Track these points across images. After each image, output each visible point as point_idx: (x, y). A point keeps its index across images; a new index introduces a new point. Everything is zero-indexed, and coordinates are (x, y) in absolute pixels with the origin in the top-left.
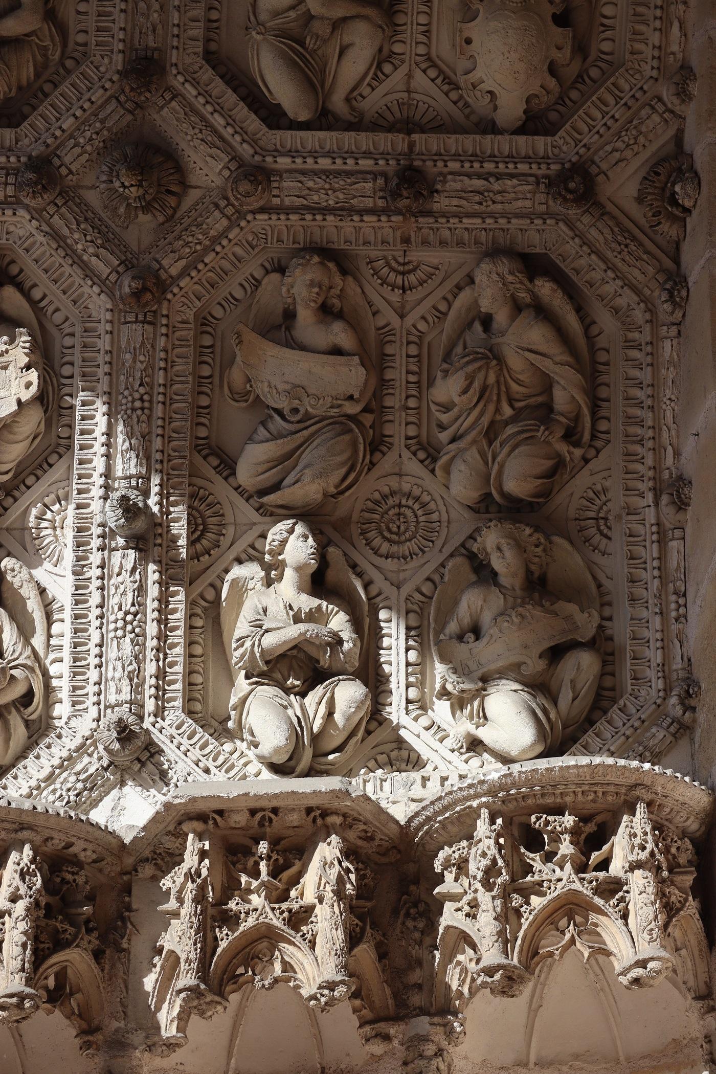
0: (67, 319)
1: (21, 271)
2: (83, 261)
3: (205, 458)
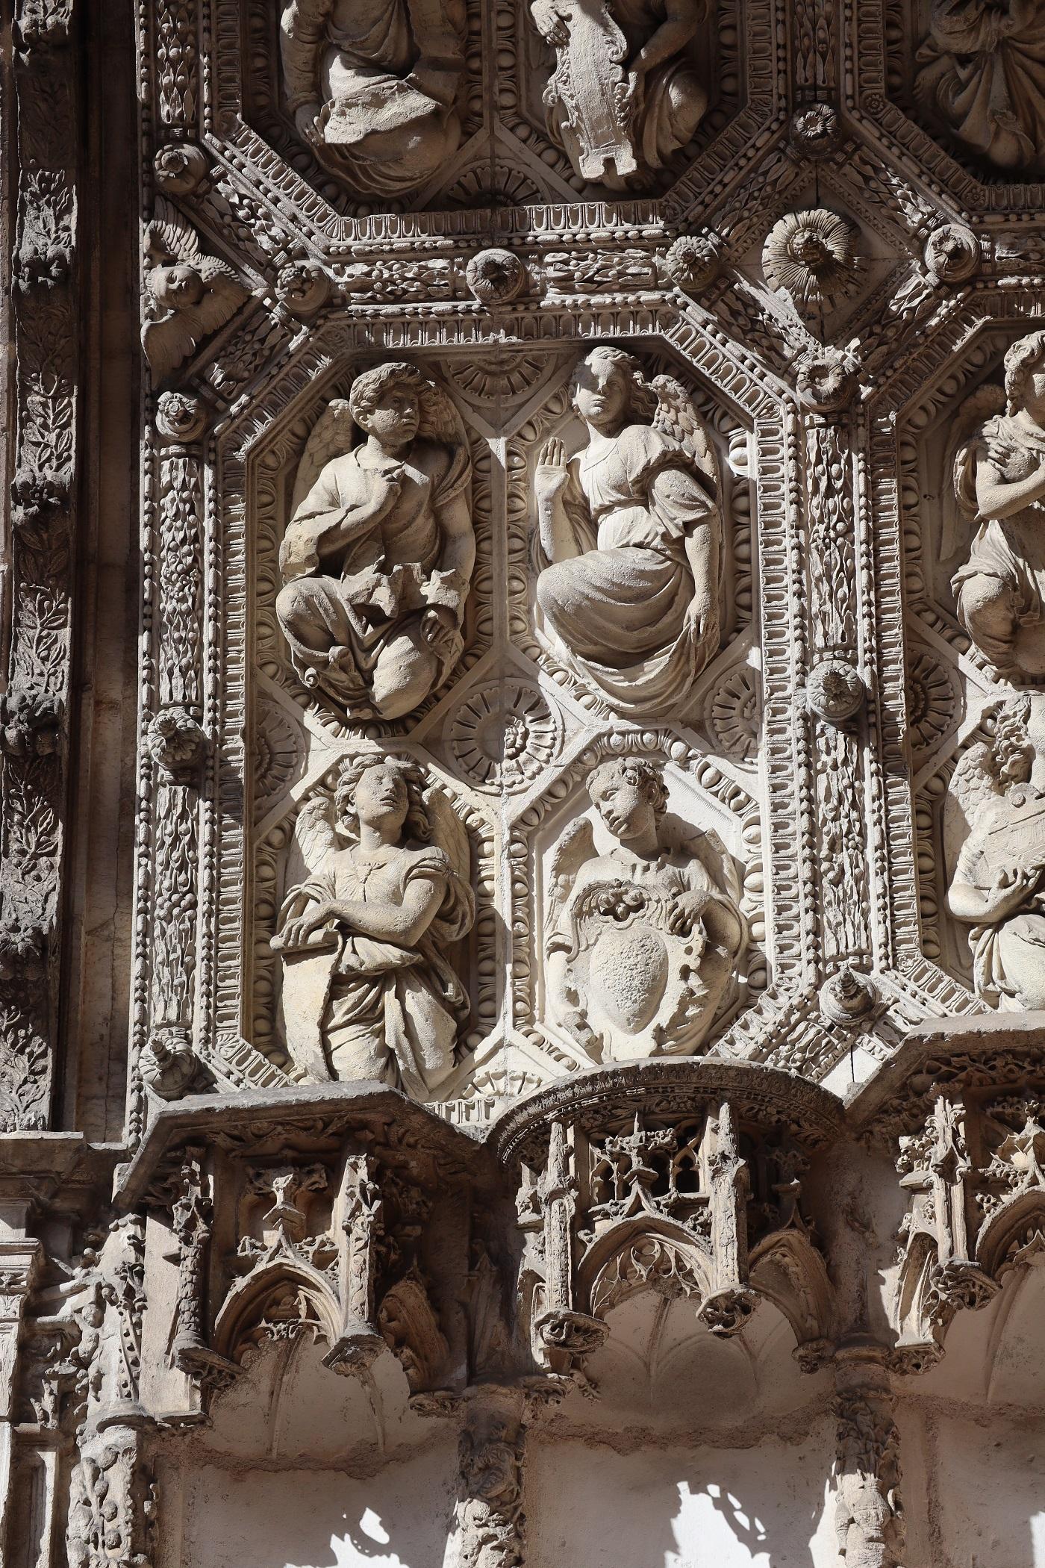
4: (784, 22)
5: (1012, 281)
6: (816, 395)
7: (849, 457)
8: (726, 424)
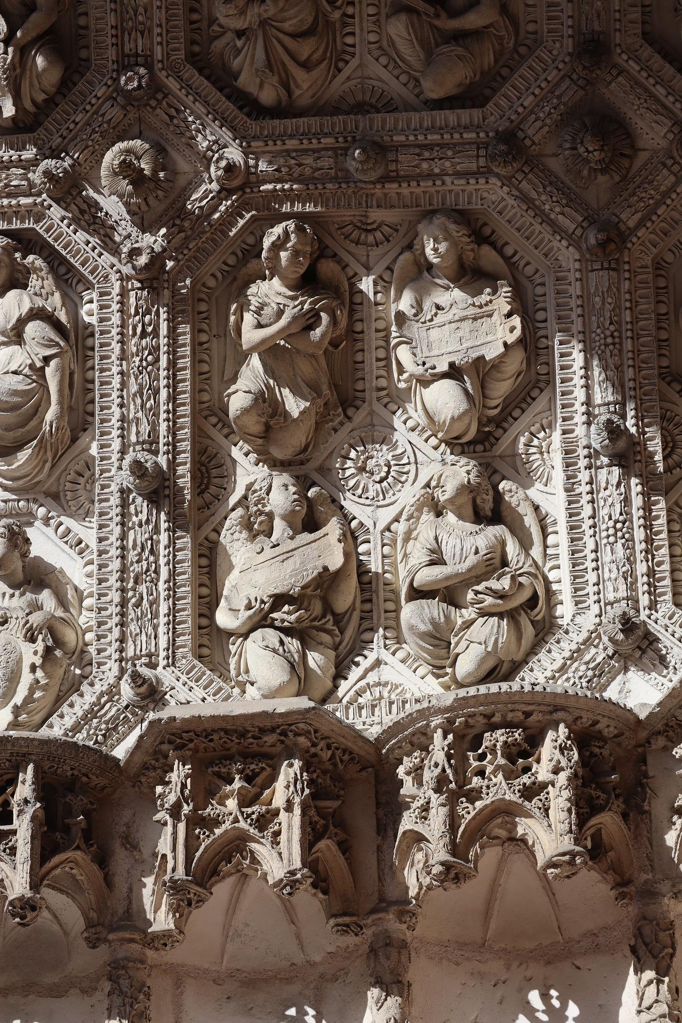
0: (537, 271)
1: (493, 232)
2: (550, 219)
3: (669, 384)
4: (115, 11)
5: (270, 187)
6: (134, 268)
7: (158, 310)
8: (80, 287)
